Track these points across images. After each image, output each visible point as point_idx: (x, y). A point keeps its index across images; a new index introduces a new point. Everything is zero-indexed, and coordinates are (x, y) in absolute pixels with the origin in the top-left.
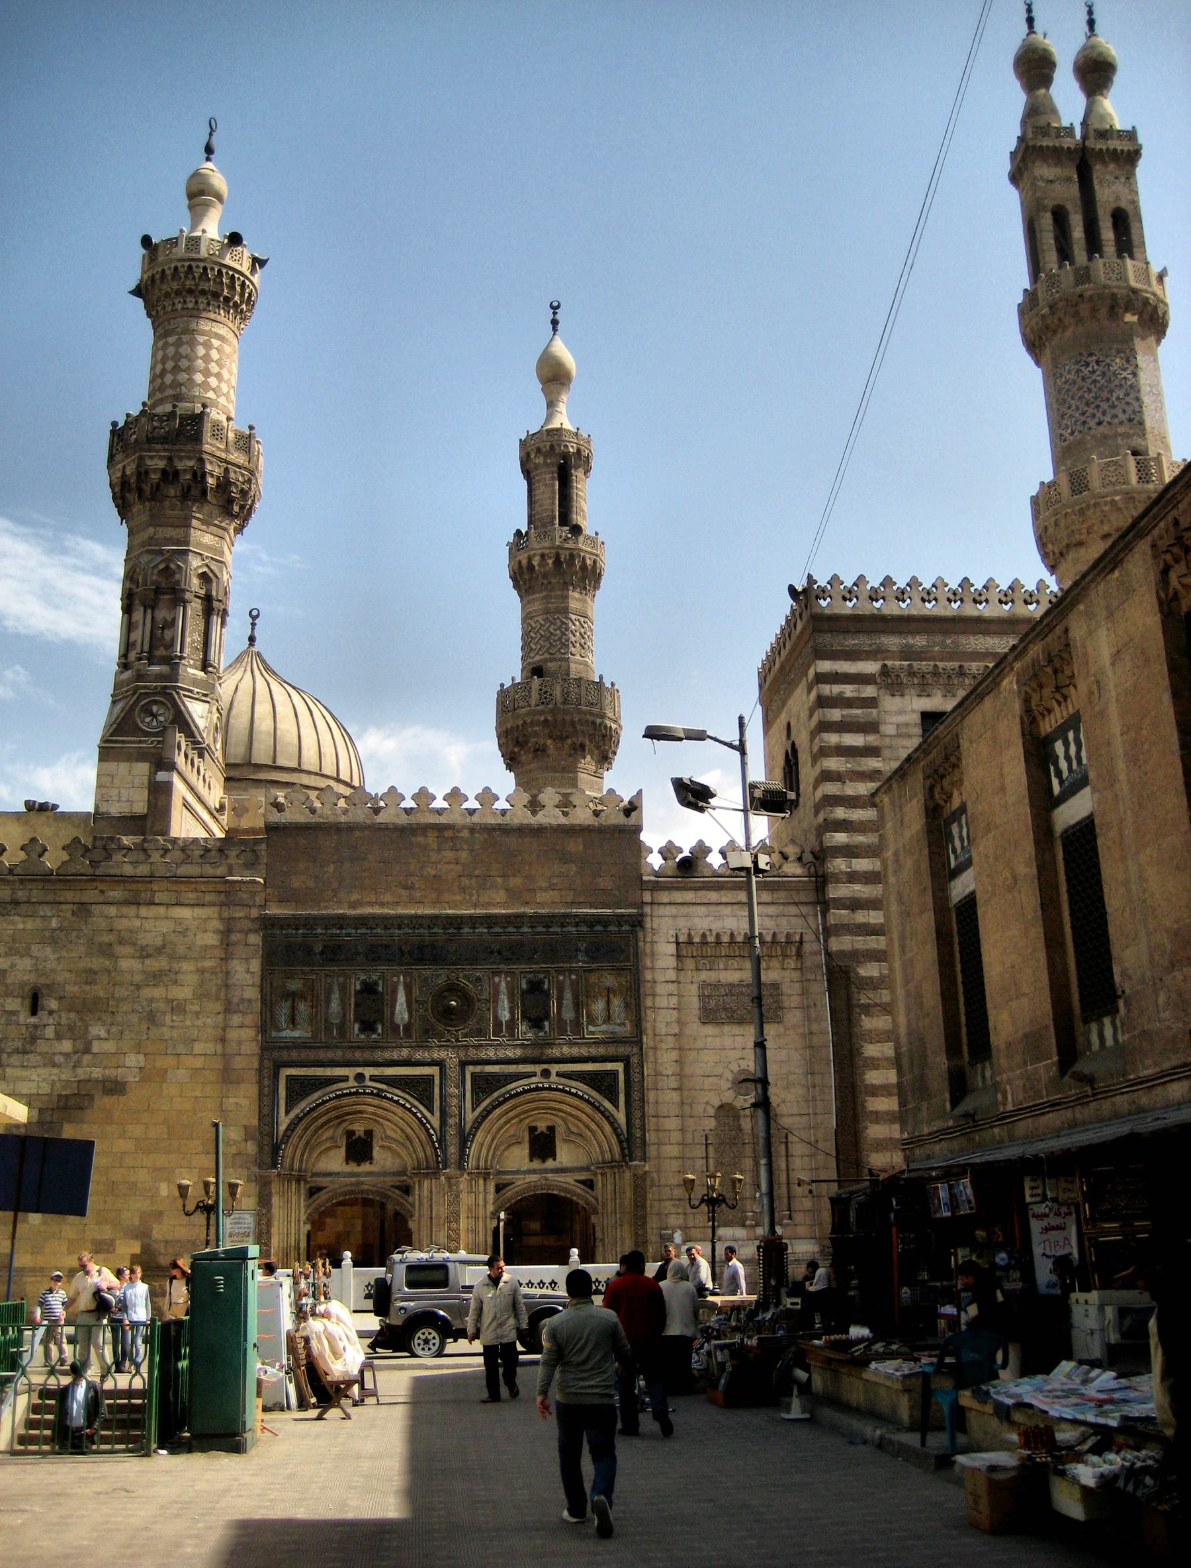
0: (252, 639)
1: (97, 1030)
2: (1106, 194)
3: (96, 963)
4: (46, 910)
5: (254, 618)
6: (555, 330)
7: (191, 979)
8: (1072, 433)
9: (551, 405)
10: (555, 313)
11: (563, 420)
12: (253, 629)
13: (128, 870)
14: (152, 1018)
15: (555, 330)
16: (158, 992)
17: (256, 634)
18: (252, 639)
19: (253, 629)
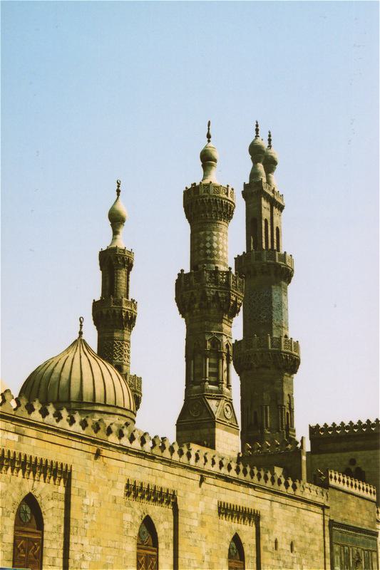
0: (81, 333)
1: (304, 561)
2: (276, 219)
3: (301, 533)
4: (292, 509)
5: (81, 322)
6: (118, 195)
7: (318, 543)
8: (266, 319)
9: (115, 233)
10: (119, 186)
11: (122, 243)
12: (81, 328)
13: (309, 497)
14: (312, 558)
15: (118, 195)
16: (312, 547)
17: (83, 330)
18: (81, 333)
19: (81, 328)
